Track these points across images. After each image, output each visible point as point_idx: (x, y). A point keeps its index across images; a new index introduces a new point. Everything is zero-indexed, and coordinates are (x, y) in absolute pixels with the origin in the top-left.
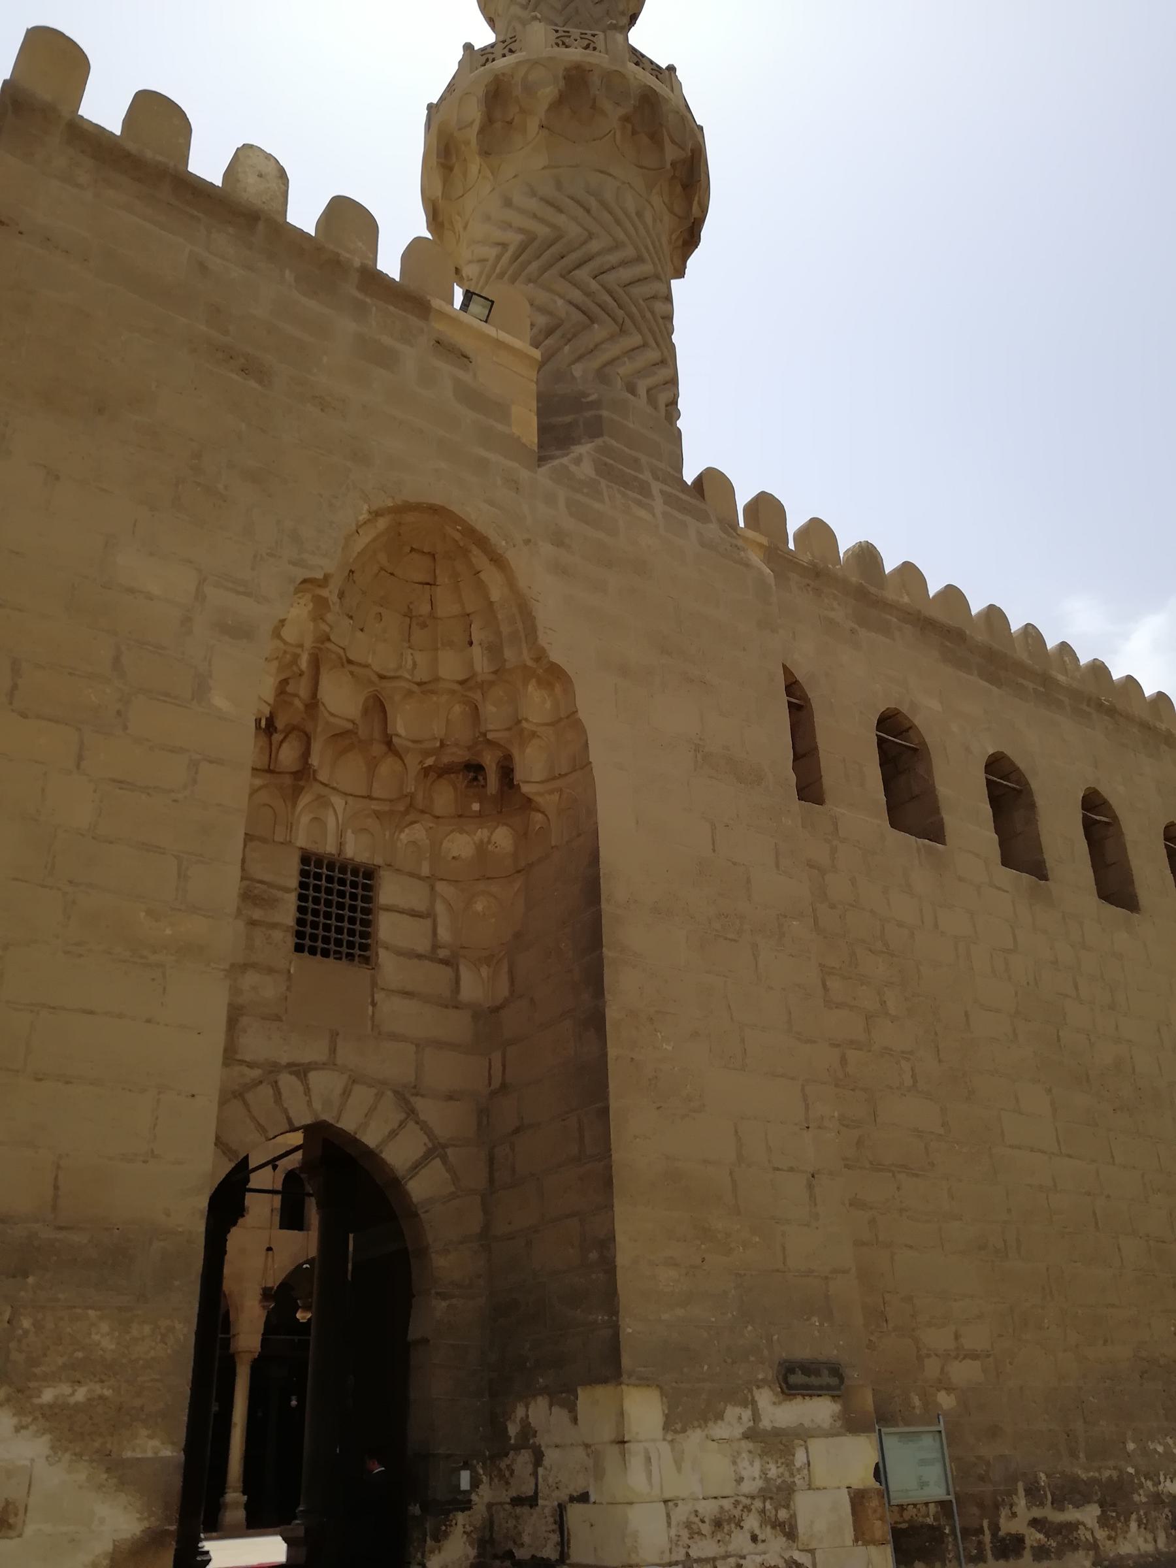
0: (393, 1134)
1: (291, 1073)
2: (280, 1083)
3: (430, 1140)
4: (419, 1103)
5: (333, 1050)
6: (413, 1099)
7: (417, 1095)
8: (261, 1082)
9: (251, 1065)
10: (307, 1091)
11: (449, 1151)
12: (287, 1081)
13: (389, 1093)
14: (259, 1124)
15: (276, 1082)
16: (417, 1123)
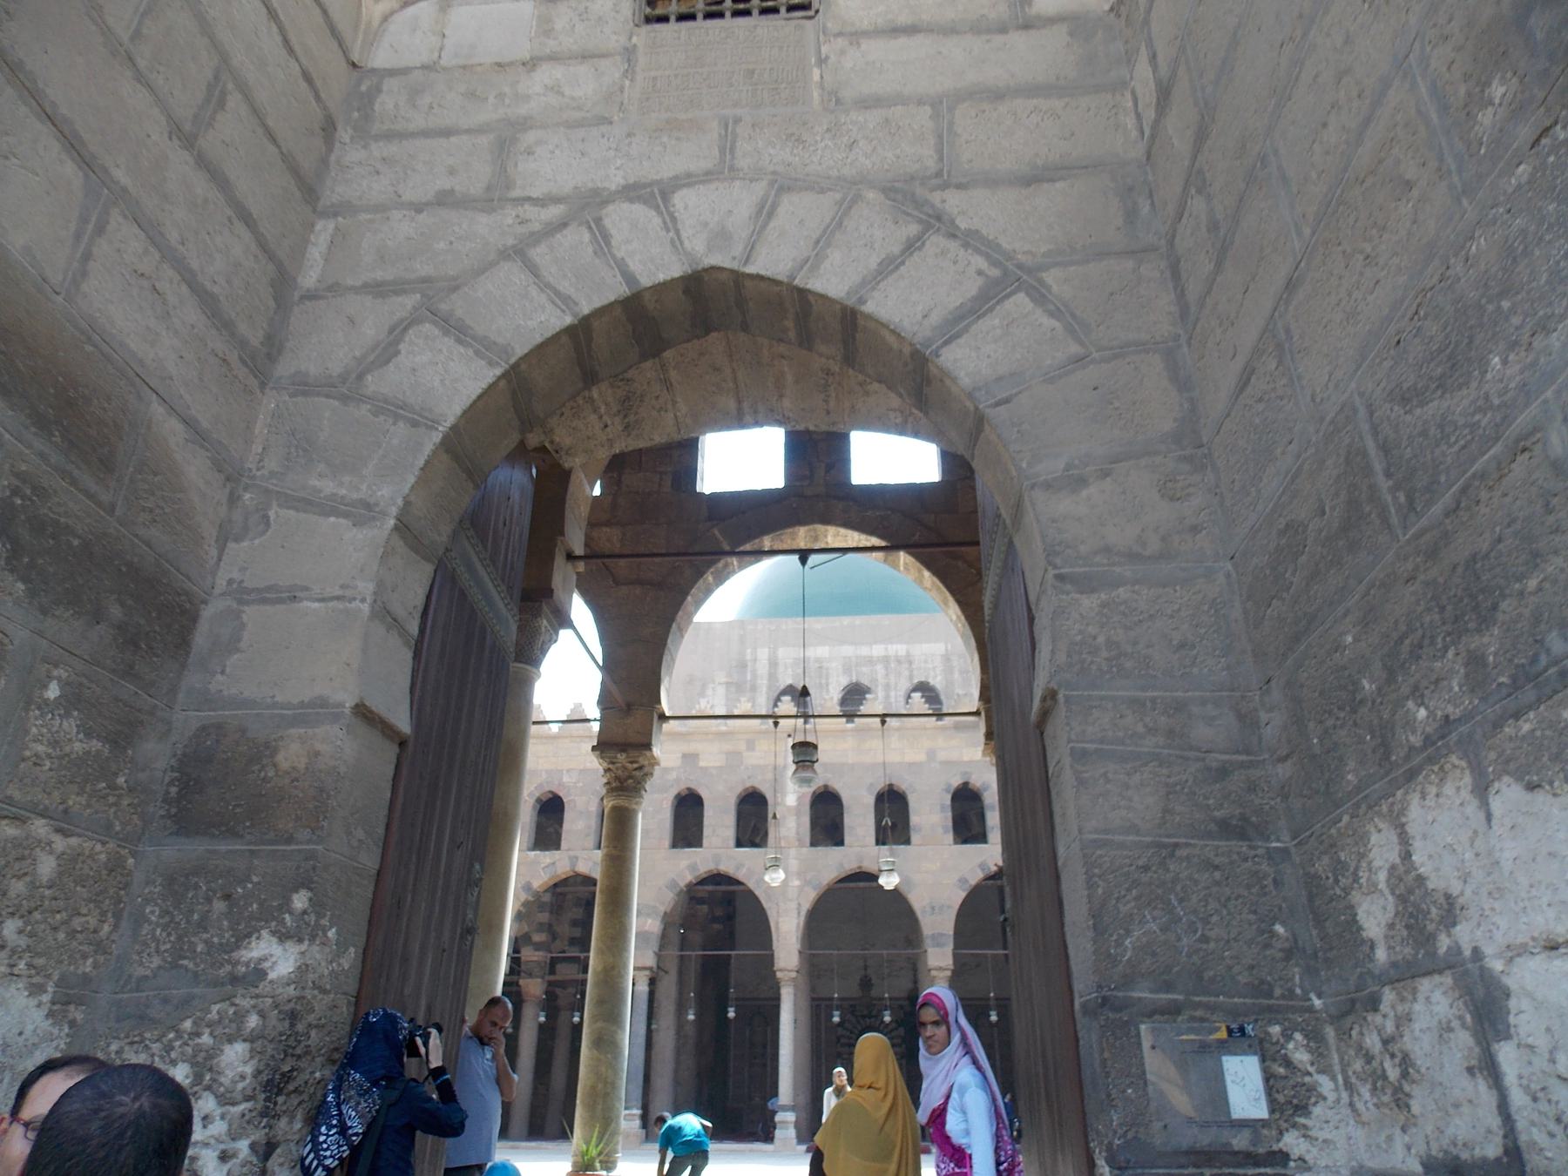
0: (889, 266)
1: (631, 201)
2: (607, 222)
3: (995, 263)
4: (952, 201)
5: (727, 146)
6: (936, 198)
7: (945, 186)
8: (565, 225)
9: (541, 202)
10: (672, 223)
11: (1050, 277)
12: (619, 218)
13: (871, 195)
14: (557, 293)
15: (598, 220)
16: (954, 236)
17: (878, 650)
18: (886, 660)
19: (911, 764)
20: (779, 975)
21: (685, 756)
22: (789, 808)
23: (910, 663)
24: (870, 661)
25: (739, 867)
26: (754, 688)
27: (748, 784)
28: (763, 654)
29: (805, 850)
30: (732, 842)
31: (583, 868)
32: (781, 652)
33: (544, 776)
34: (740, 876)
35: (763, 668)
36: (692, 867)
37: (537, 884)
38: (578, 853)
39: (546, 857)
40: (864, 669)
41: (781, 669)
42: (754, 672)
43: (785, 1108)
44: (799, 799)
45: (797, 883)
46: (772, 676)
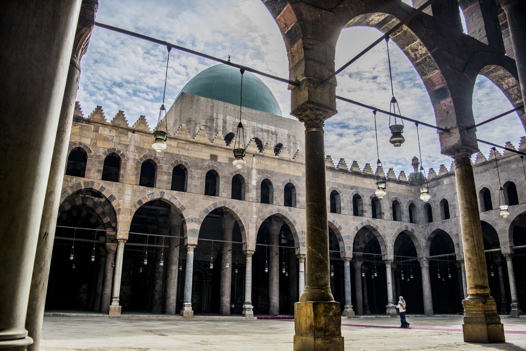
17: (265, 127)
18: (267, 131)
19: (297, 177)
20: (248, 252)
21: (212, 156)
22: (253, 186)
23: (276, 135)
24: (262, 130)
25: (234, 207)
26: (217, 131)
27: (238, 173)
28: (221, 117)
29: (259, 204)
30: (230, 197)
31: (166, 197)
32: (228, 118)
33: (147, 152)
34: (234, 210)
35: (220, 123)
36: (215, 204)
37: (144, 202)
38: (164, 191)
39: (149, 191)
40: (260, 133)
41: (228, 125)
42: (217, 125)
43: (248, 303)
44: (257, 183)
45: (255, 217)
46: (224, 127)
